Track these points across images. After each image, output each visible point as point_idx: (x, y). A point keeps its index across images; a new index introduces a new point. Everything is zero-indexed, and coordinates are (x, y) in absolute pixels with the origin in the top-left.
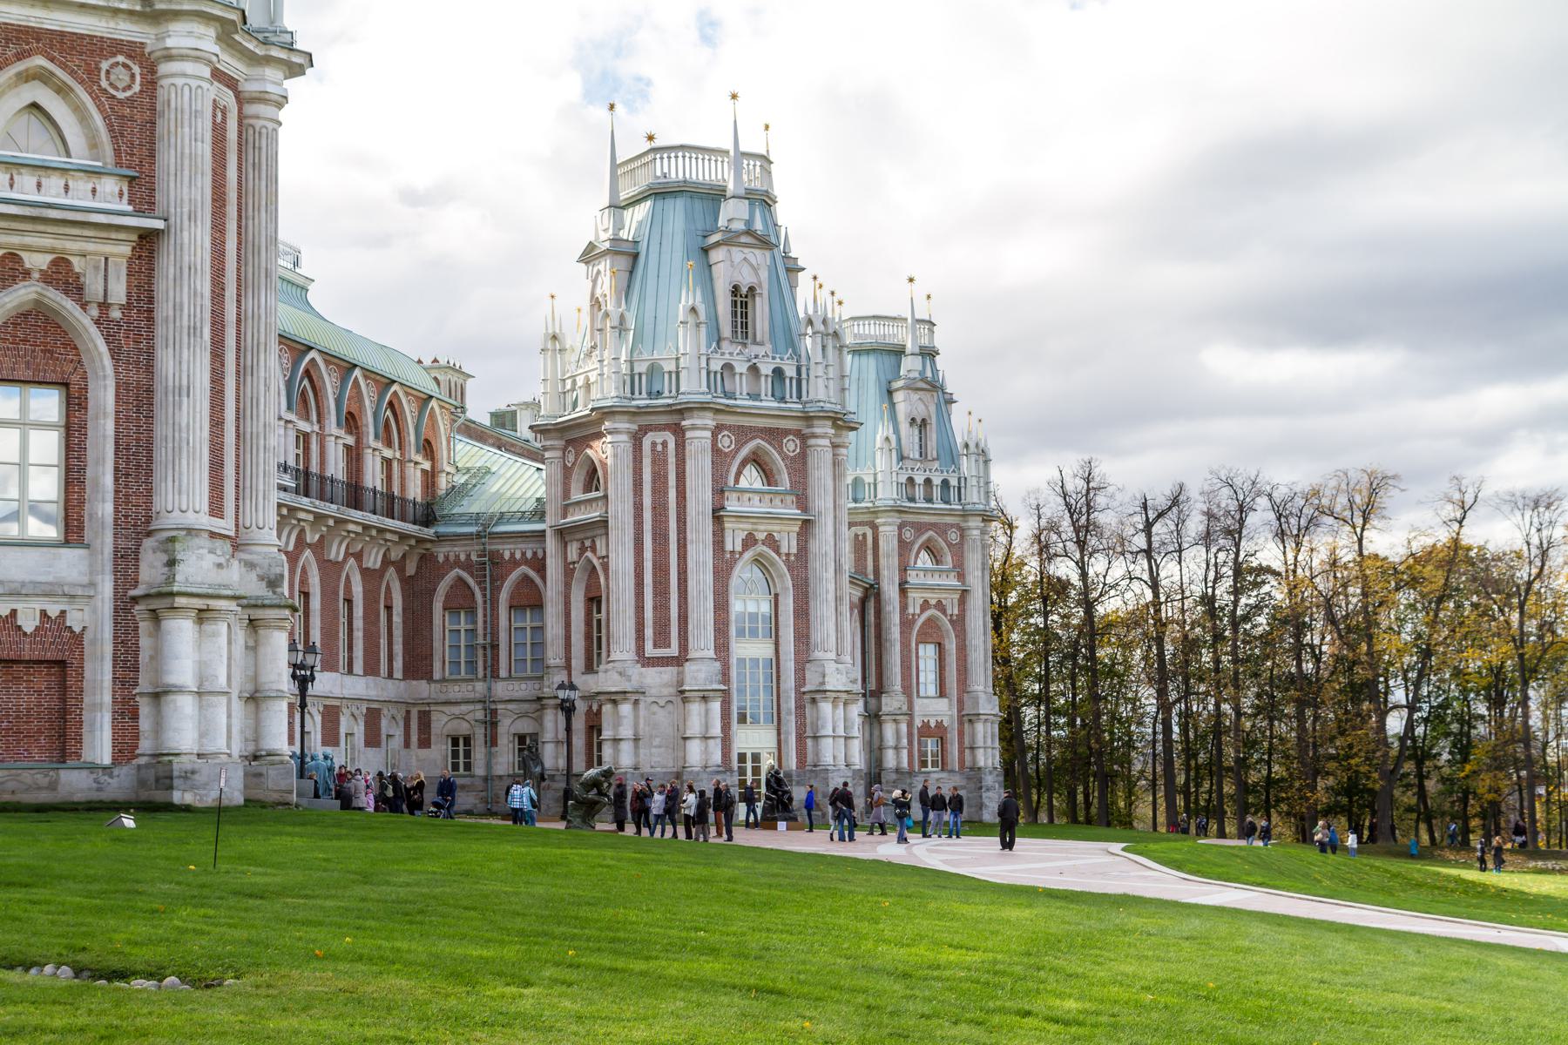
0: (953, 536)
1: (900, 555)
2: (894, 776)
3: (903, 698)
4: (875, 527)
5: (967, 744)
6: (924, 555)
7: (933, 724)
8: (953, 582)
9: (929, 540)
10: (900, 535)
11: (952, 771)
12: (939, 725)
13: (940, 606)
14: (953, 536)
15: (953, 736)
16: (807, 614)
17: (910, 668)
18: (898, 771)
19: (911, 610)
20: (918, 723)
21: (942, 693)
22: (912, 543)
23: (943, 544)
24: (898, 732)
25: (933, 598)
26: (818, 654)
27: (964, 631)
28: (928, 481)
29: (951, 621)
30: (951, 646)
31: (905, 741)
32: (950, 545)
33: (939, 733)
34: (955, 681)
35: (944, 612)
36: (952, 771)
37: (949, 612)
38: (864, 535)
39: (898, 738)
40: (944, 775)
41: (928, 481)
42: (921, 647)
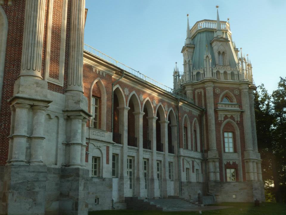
0: (237, 92)
1: (214, 99)
2: (214, 184)
3: (216, 152)
4: (204, 89)
5: (246, 171)
6: (225, 99)
7: (231, 163)
8: (237, 108)
9: (227, 93)
10: (214, 91)
11: (241, 182)
12: (234, 163)
13: (232, 118)
14: (237, 92)
15: (240, 168)
16: (20, 44)
17: (220, 141)
18: (216, 181)
19: (220, 119)
20: (225, 162)
21: (235, 151)
22: (219, 94)
23: (233, 95)
24: (215, 166)
25: (229, 114)
26: (23, 72)
27: (243, 127)
28: (225, 73)
29: (237, 124)
30: (238, 133)
31: (218, 170)
32: (235, 95)
33: (234, 166)
34: (240, 146)
35: (234, 120)
36: (241, 182)
37: (236, 120)
38: (201, 92)
39: (215, 168)
40: (237, 183)
41: (225, 73)
42: (226, 134)
